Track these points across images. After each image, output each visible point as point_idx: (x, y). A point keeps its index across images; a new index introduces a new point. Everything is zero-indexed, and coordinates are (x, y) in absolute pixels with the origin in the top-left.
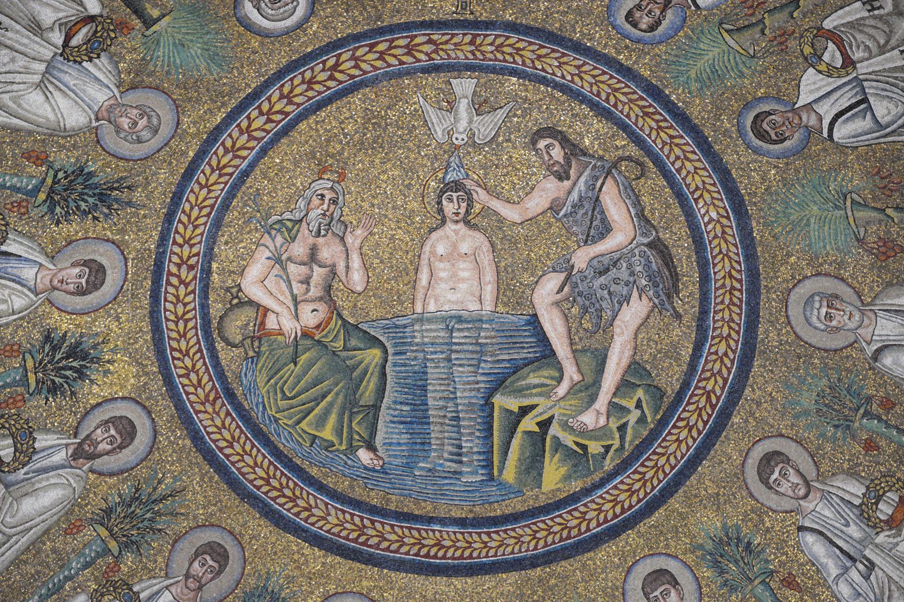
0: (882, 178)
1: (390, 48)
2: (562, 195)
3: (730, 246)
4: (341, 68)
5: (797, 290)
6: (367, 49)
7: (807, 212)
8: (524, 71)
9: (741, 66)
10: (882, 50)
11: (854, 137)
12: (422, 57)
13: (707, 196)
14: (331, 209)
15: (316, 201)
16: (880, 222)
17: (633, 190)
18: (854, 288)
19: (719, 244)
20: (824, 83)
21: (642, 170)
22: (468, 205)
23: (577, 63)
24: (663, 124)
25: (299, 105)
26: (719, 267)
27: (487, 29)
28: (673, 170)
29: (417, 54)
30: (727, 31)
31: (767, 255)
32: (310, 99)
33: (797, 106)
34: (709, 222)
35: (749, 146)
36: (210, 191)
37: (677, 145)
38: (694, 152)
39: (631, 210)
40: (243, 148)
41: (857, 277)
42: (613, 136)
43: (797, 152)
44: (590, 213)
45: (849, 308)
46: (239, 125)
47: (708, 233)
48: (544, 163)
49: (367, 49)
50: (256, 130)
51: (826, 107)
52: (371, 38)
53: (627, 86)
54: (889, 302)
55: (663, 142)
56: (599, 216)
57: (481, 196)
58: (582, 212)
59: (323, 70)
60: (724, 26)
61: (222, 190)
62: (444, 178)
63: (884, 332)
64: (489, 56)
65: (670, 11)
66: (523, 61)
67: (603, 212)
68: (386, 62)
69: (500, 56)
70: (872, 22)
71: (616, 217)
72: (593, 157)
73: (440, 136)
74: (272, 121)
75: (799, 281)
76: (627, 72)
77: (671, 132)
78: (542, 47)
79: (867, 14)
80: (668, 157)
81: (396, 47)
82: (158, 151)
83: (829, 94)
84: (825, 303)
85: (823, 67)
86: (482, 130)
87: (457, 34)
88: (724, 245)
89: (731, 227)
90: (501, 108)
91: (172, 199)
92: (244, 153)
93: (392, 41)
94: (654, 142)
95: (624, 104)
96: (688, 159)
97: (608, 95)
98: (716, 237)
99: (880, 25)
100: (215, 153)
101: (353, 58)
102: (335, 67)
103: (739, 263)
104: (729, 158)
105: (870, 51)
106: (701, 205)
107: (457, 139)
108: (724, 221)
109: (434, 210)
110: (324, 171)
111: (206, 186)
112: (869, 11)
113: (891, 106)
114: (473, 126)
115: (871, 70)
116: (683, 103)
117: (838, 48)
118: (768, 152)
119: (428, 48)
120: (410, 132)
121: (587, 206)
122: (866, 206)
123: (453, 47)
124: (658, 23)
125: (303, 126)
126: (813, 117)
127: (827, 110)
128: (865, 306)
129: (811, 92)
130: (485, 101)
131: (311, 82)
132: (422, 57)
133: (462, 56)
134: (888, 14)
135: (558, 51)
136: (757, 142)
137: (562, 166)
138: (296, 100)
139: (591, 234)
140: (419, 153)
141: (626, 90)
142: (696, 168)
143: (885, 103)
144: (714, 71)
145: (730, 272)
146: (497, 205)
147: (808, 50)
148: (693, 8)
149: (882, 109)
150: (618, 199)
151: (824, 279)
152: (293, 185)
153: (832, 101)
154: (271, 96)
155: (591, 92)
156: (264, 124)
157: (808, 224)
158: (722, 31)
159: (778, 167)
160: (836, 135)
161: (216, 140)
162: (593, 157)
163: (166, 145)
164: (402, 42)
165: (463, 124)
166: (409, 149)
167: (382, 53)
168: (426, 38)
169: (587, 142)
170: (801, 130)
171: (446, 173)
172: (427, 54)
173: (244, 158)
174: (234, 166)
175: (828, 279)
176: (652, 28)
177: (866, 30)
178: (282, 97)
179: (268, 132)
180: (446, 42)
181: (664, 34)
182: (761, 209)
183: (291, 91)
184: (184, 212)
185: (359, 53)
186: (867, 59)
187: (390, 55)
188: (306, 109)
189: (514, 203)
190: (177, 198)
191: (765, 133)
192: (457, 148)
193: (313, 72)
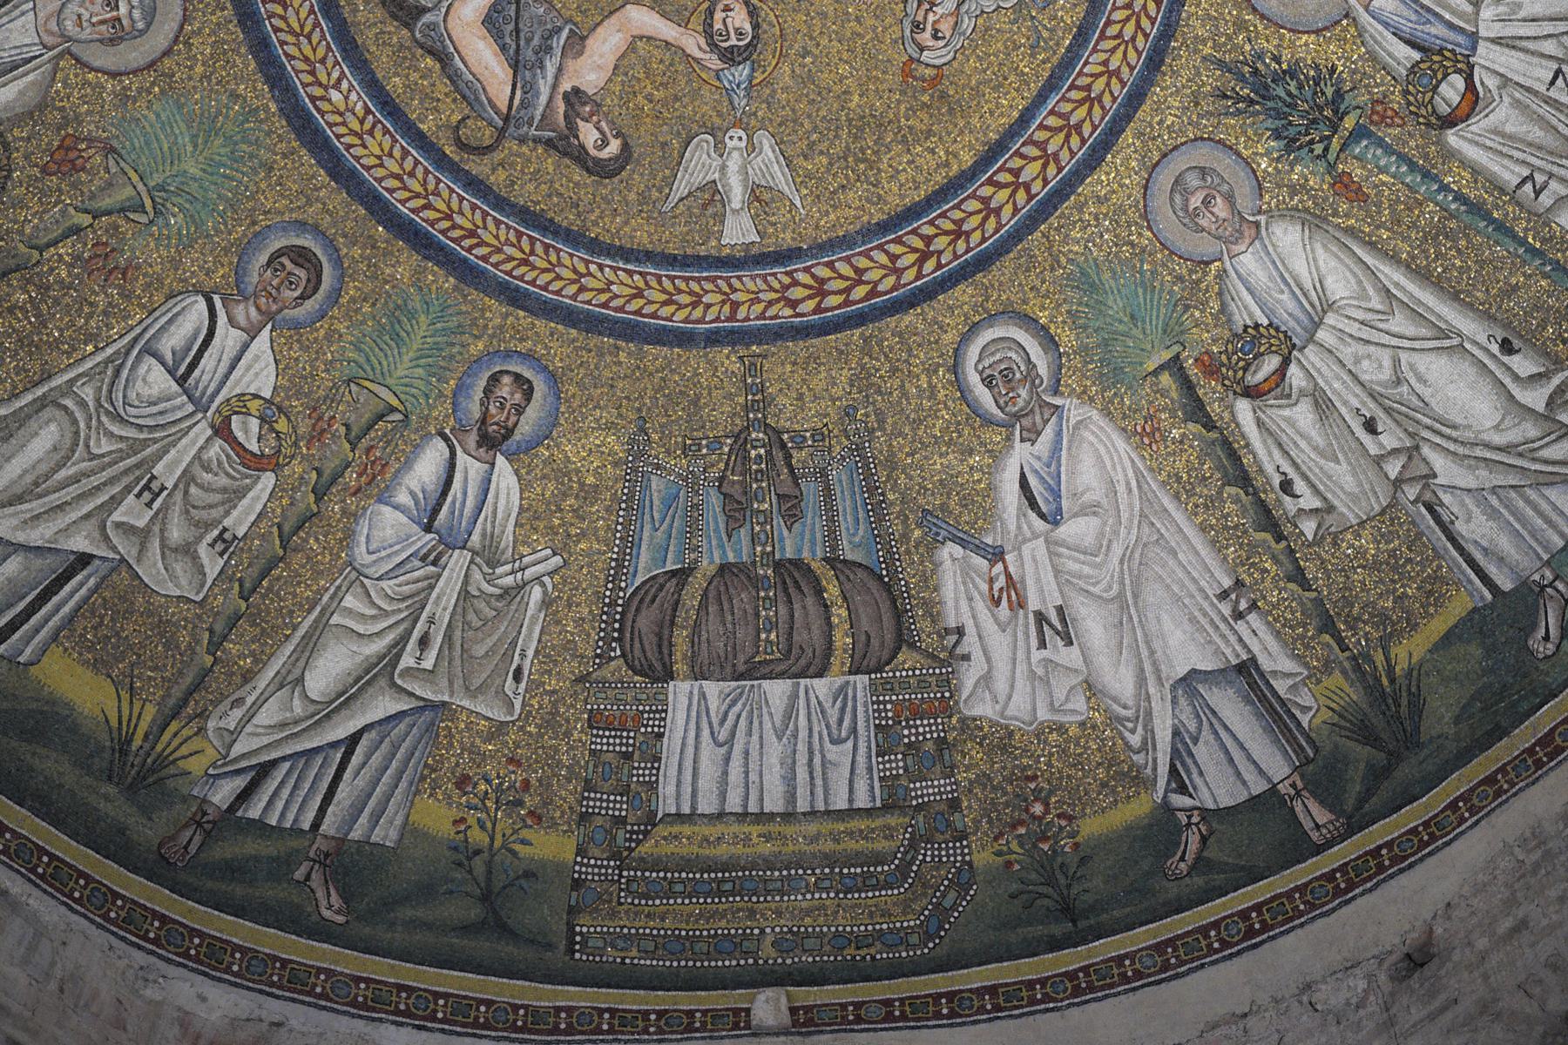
0: (116, 268)
1: (848, 290)
2: (571, 64)
3: (297, 54)
4: (912, 258)
5: (175, 26)
6: (880, 288)
7: (201, 159)
8: (657, 265)
9: (362, 360)
10: (187, 478)
11: (178, 314)
12: (802, 277)
13: (356, 126)
14: (921, 13)
15: (946, 28)
16: (93, 197)
17: (464, 97)
18: (92, 69)
19: (314, 50)
20: (246, 379)
21: (459, 138)
22: (711, 26)
23: (586, 296)
24: (445, 224)
25: (973, 196)
26: (303, 14)
27: (717, 331)
28: (414, 152)
29: (812, 282)
30: (393, 410)
31: (238, 61)
32: (958, 207)
33: (269, 326)
34: (339, 81)
35: (316, 230)
36: (1105, 63)
37: (418, 196)
38: (391, 191)
39: (461, 66)
40: (1055, 130)
41: (93, 89)
42: (513, 183)
43: (244, 251)
44: (522, 43)
45: (84, 36)
46: (1060, 170)
47: (337, 63)
48: (606, 115)
49: (880, 288)
50: (1035, 159)
51: (230, 342)
52: (874, 308)
53: (509, 273)
54: (31, 77)
55: (438, 195)
56: (508, 40)
57: (693, 43)
58: (536, 41)
59: (940, 253)
60: (398, 417)
61: (1086, 63)
62: (753, 70)
63: (19, 22)
64: (708, 286)
65: (477, 415)
66: (660, 283)
67: (503, 48)
68: (852, 266)
69: (695, 287)
70: (215, 513)
71: (481, 45)
72: (534, 141)
73: (765, 141)
74: (1010, 171)
75: (176, 41)
76: (514, 297)
77: (431, 215)
78: (638, 312)
79: (227, 522)
80: (427, 172)
81: (839, 292)
82: (1175, 148)
83: (232, 367)
84: (125, 22)
85: (254, 405)
86: (705, 156)
87: (757, 318)
88: (307, 50)
89: (305, 85)
90: (682, 199)
91: (1162, 62)
92: (1052, 121)
93: (847, 303)
94: (452, 191)
95: (508, 242)
96: (397, 177)
97: (532, 253)
98: (323, 61)
99: (203, 514)
100: (1095, 128)
101: (899, 272)
102: (924, 257)
103: (277, 30)
104: (337, 199)
105: (203, 467)
106: (359, 108)
107: (740, 139)
108: (318, 92)
109: (763, 14)
110: (936, 80)
111: (1111, 74)
112: (225, 530)
113: (145, 392)
114: (717, 162)
115: (192, 434)
116: (426, 268)
117: (245, 450)
118: (284, 229)
119: (797, 293)
120: (811, 145)
121: (528, 54)
122: (122, 210)
123: (761, 295)
124: (488, 391)
125: (967, 159)
126: (241, 320)
127: (228, 338)
128: (66, 53)
129: (257, 358)
130: (705, 207)
131: (958, 233)
132: (802, 277)
133: (748, 281)
134: (199, 539)
135: (616, 310)
136: (306, 241)
137: (578, 115)
138: (974, 205)
139: (514, 7)
140: (793, 110)
141: (508, 267)
142: (381, 165)
143: (155, 391)
144: (396, 337)
145: (285, 9)
146: (668, 30)
147: (282, 425)
148: (447, 431)
149: (155, 380)
150: (484, 75)
151: (142, 62)
152: (979, 59)
153: (225, 357)
154: (1014, 215)
155: (558, 251)
156: (1022, 168)
157: (194, 137)
158: (401, 408)
159: (265, 213)
160: (202, 305)
161: (1093, 148)
162: (536, 140)
163: (1165, 155)
164: (833, 300)
165: (734, 163)
166: (809, 116)
167: (860, 282)
168: (801, 308)
169: (549, 165)
170: (250, 289)
171: (751, 78)
172: (795, 283)
173: (1052, 112)
174: (1069, 100)
175: (136, 65)
176: (495, 379)
177: (218, 497)
178: (998, 212)
179: (1017, 153)
180: (770, 303)
181: (476, 375)
182: (269, 134)
183: (985, 219)
184: (1146, 36)
185: (890, 281)
186: (202, 448)
187: (847, 279)
188: (963, 187)
189: (641, 38)
190: (1155, 62)
191: (301, 261)
192: (737, 124)
193: (955, 252)
